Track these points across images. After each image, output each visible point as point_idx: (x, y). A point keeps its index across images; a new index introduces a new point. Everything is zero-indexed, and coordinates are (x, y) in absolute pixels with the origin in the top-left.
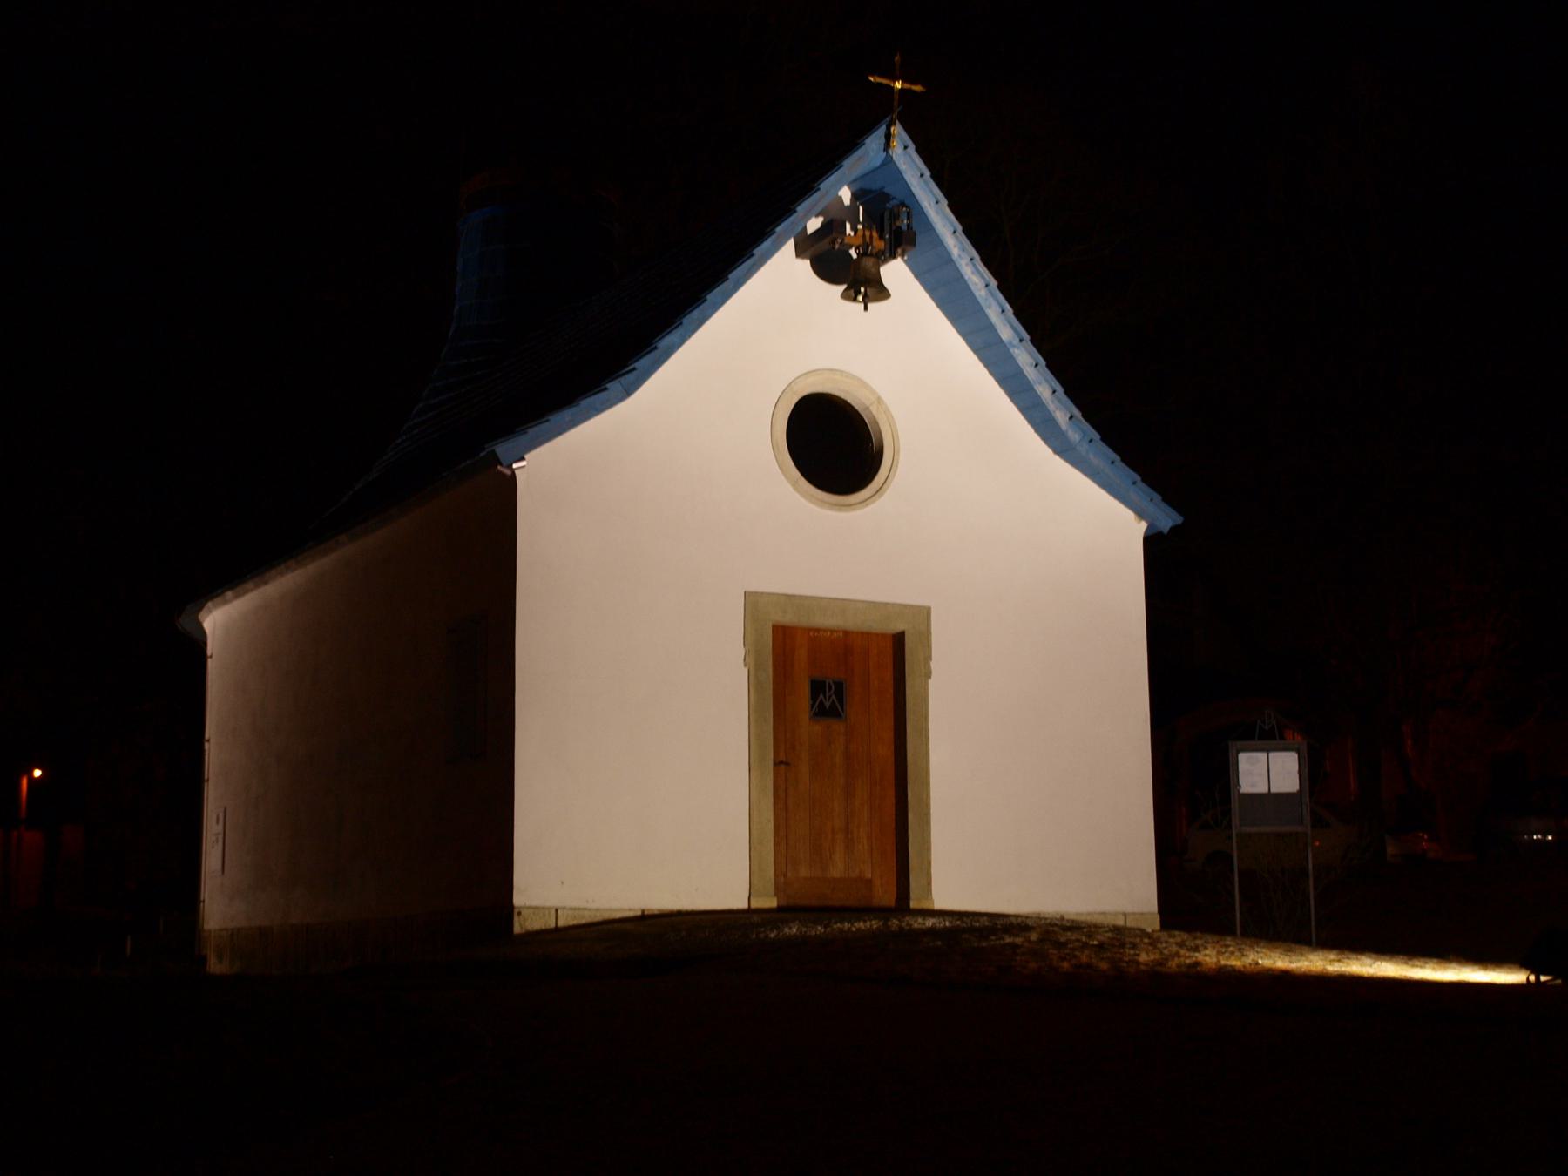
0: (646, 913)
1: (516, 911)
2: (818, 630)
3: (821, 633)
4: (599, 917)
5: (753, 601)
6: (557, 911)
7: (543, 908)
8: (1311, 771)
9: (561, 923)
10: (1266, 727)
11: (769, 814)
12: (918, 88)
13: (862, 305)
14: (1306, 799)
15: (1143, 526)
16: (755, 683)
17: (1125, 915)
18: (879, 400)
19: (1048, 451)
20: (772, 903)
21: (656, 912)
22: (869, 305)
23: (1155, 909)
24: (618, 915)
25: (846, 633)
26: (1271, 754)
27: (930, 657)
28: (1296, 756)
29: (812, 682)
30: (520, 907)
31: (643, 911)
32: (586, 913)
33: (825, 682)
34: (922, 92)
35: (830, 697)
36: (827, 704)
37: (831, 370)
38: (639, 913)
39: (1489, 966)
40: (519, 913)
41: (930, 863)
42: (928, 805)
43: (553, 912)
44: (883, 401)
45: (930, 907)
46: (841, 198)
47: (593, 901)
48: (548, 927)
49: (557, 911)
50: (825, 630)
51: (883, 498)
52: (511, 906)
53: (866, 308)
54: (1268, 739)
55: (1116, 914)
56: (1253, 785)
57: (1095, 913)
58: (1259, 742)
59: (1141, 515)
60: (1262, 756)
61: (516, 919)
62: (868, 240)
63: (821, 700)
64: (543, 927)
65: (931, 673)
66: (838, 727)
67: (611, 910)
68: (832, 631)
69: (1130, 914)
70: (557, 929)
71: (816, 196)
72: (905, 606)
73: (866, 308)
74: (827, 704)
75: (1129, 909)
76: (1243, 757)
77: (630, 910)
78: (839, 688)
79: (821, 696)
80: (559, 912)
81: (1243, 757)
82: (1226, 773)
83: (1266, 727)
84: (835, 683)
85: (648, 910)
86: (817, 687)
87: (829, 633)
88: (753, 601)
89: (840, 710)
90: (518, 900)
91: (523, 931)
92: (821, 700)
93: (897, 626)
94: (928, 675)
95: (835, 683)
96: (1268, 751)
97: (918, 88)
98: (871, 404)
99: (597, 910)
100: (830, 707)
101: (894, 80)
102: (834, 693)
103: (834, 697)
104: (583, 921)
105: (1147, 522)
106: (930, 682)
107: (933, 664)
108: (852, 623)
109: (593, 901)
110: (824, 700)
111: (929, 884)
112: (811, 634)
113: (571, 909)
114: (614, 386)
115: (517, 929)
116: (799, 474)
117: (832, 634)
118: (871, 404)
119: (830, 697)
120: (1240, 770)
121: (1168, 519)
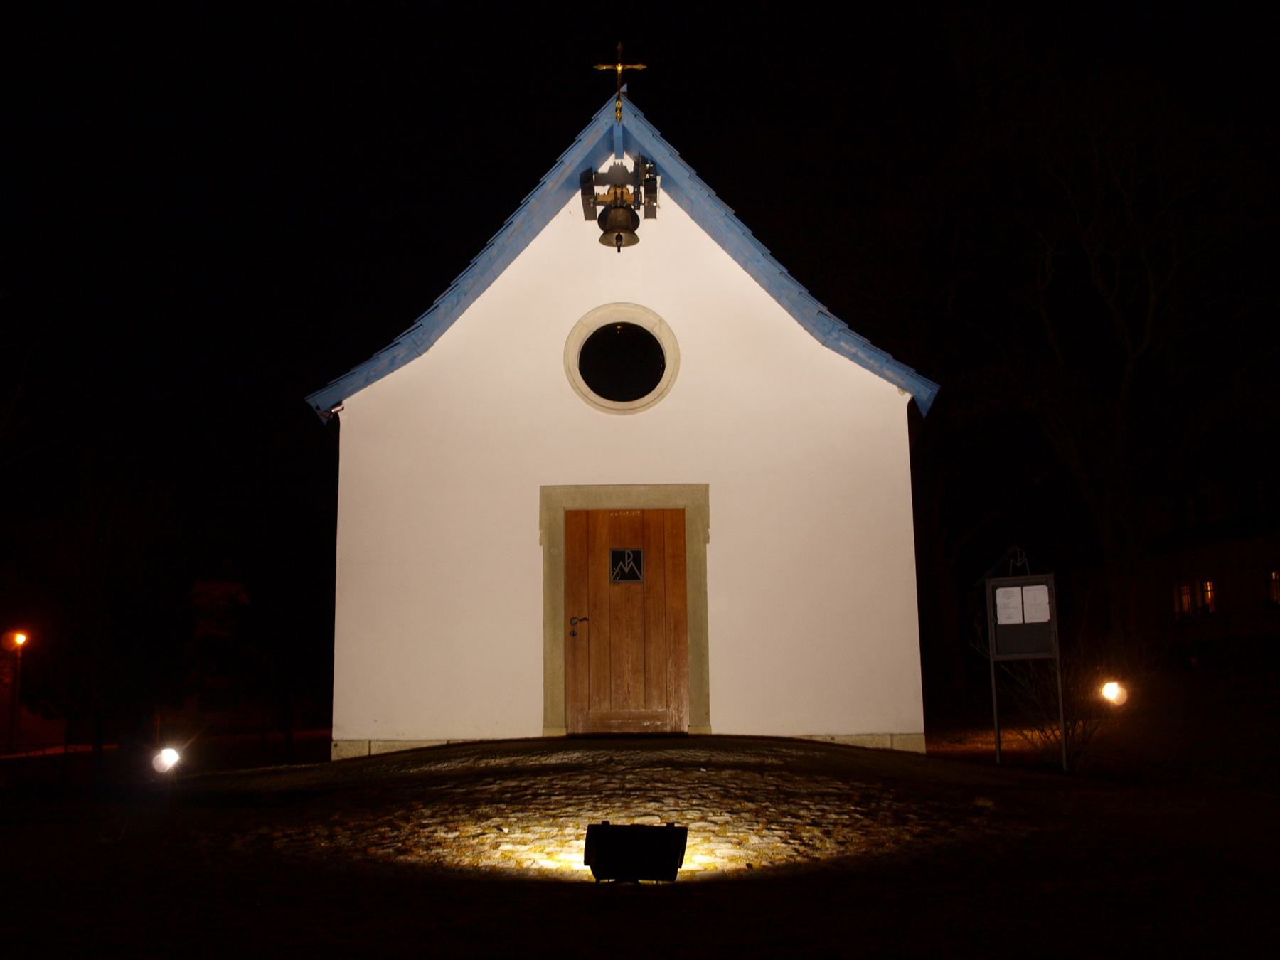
0: (451, 742)
1: (333, 743)
2: (618, 511)
3: (621, 513)
4: (408, 747)
5: (547, 494)
6: (370, 742)
7: (359, 741)
8: (1059, 603)
9: (374, 752)
10: (1019, 564)
11: (560, 662)
12: (639, 67)
13: (616, 249)
14: (1055, 628)
15: (908, 397)
16: (549, 559)
17: (892, 735)
18: (661, 321)
19: (817, 344)
20: (562, 732)
21: (460, 742)
22: (621, 249)
23: (923, 732)
24: (425, 745)
25: (643, 511)
26: (1025, 588)
27: (708, 526)
28: (1047, 588)
29: (613, 552)
30: (337, 741)
31: (448, 741)
32: (397, 744)
33: (624, 552)
34: (644, 70)
35: (629, 564)
36: (627, 570)
37: (617, 303)
38: (445, 743)
39: (515, 873)
40: (336, 745)
41: (708, 696)
42: (706, 648)
43: (367, 744)
44: (664, 321)
45: (708, 733)
46: (625, 167)
47: (403, 734)
48: (361, 755)
49: (370, 742)
50: (624, 511)
51: (664, 400)
52: (329, 739)
53: (619, 251)
54: (1021, 576)
55: (884, 735)
56: (1008, 618)
57: (863, 735)
58: (1012, 578)
59: (903, 389)
60: (1017, 590)
61: (333, 748)
62: (619, 195)
63: (621, 566)
64: (357, 755)
65: (709, 538)
66: (635, 587)
67: (420, 741)
68: (631, 511)
69: (896, 735)
70: (370, 757)
71: (563, 167)
72: (684, 485)
73: (619, 251)
74: (627, 570)
75: (895, 731)
76: (1000, 592)
77: (437, 740)
78: (637, 557)
79: (621, 563)
80: (372, 744)
81: (1000, 592)
82: (986, 607)
83: (1019, 564)
84: (633, 552)
85: (453, 740)
86: (617, 557)
87: (627, 513)
88: (547, 494)
89: (639, 575)
90: (336, 735)
91: (340, 758)
92: (621, 566)
93: (680, 503)
94: (706, 540)
95: (633, 552)
96: (1022, 586)
97: (639, 67)
98: (654, 326)
99: (407, 741)
100: (629, 572)
101: (615, 64)
102: (633, 560)
103: (632, 563)
104: (394, 750)
105: (910, 392)
106: (708, 546)
107: (710, 531)
108: (637, 503)
109: (403, 734)
110: (623, 567)
111: (707, 713)
112: (612, 514)
113: (384, 741)
114: (406, 340)
115: (335, 756)
116: (588, 389)
117: (629, 513)
118: (654, 326)
119: (629, 564)
120: (998, 604)
121: (927, 392)
